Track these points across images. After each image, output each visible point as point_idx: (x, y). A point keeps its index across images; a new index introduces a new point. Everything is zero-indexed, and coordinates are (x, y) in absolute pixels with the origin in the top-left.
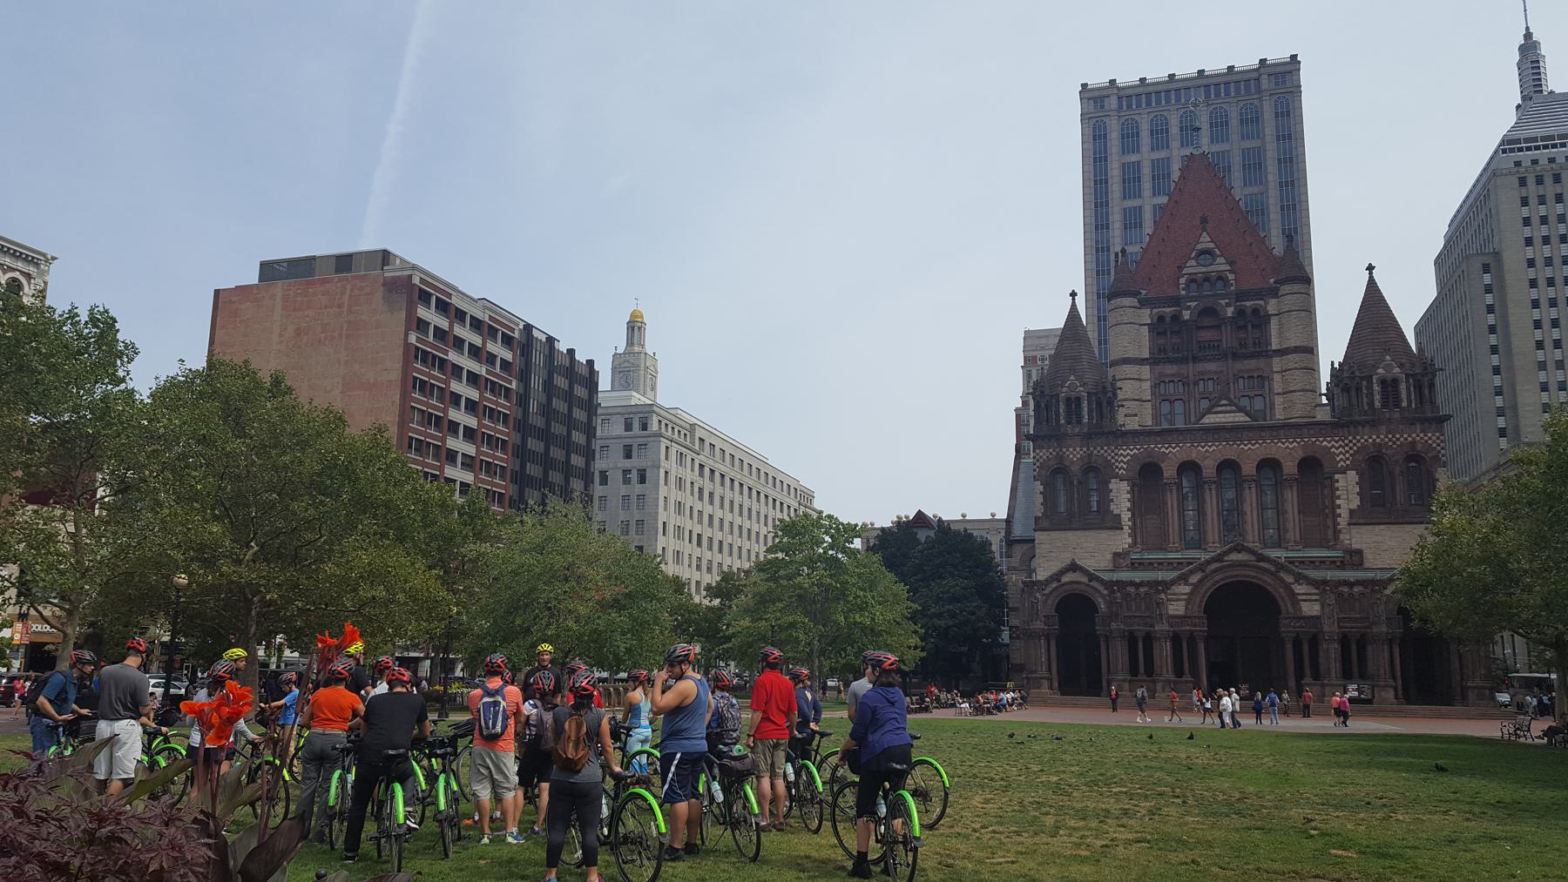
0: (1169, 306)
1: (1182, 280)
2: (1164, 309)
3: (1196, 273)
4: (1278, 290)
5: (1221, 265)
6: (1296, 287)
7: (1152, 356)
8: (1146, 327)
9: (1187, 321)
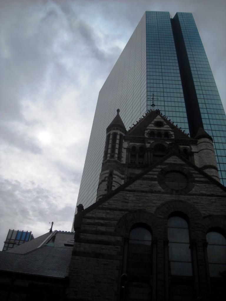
0: (138, 142)
1: (147, 131)
2: (136, 144)
3: (154, 130)
4: (197, 142)
5: (166, 127)
6: (207, 140)
7: (127, 163)
8: (126, 150)
9: (148, 148)
